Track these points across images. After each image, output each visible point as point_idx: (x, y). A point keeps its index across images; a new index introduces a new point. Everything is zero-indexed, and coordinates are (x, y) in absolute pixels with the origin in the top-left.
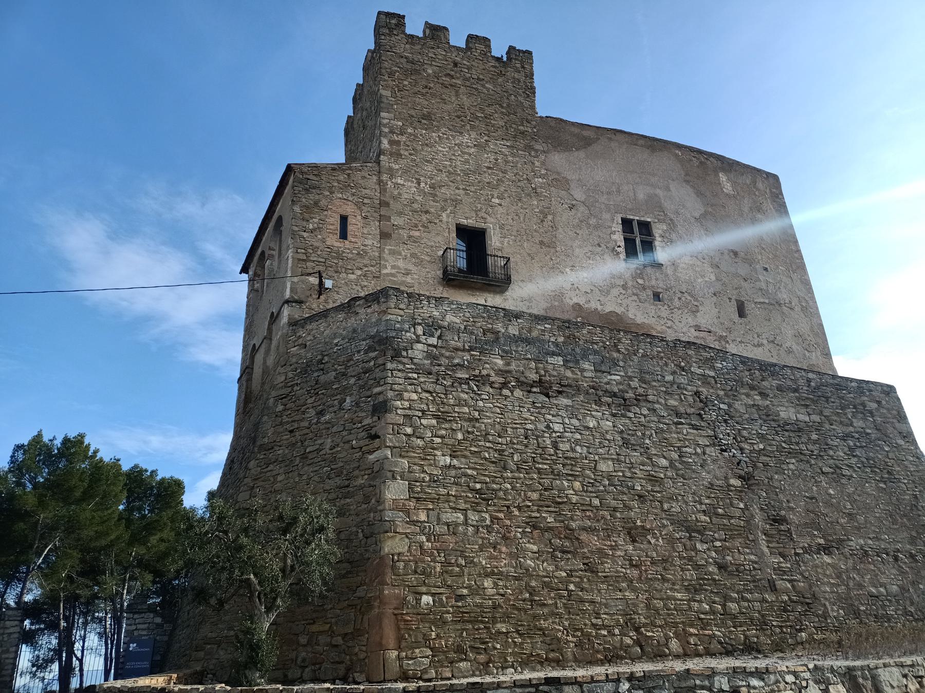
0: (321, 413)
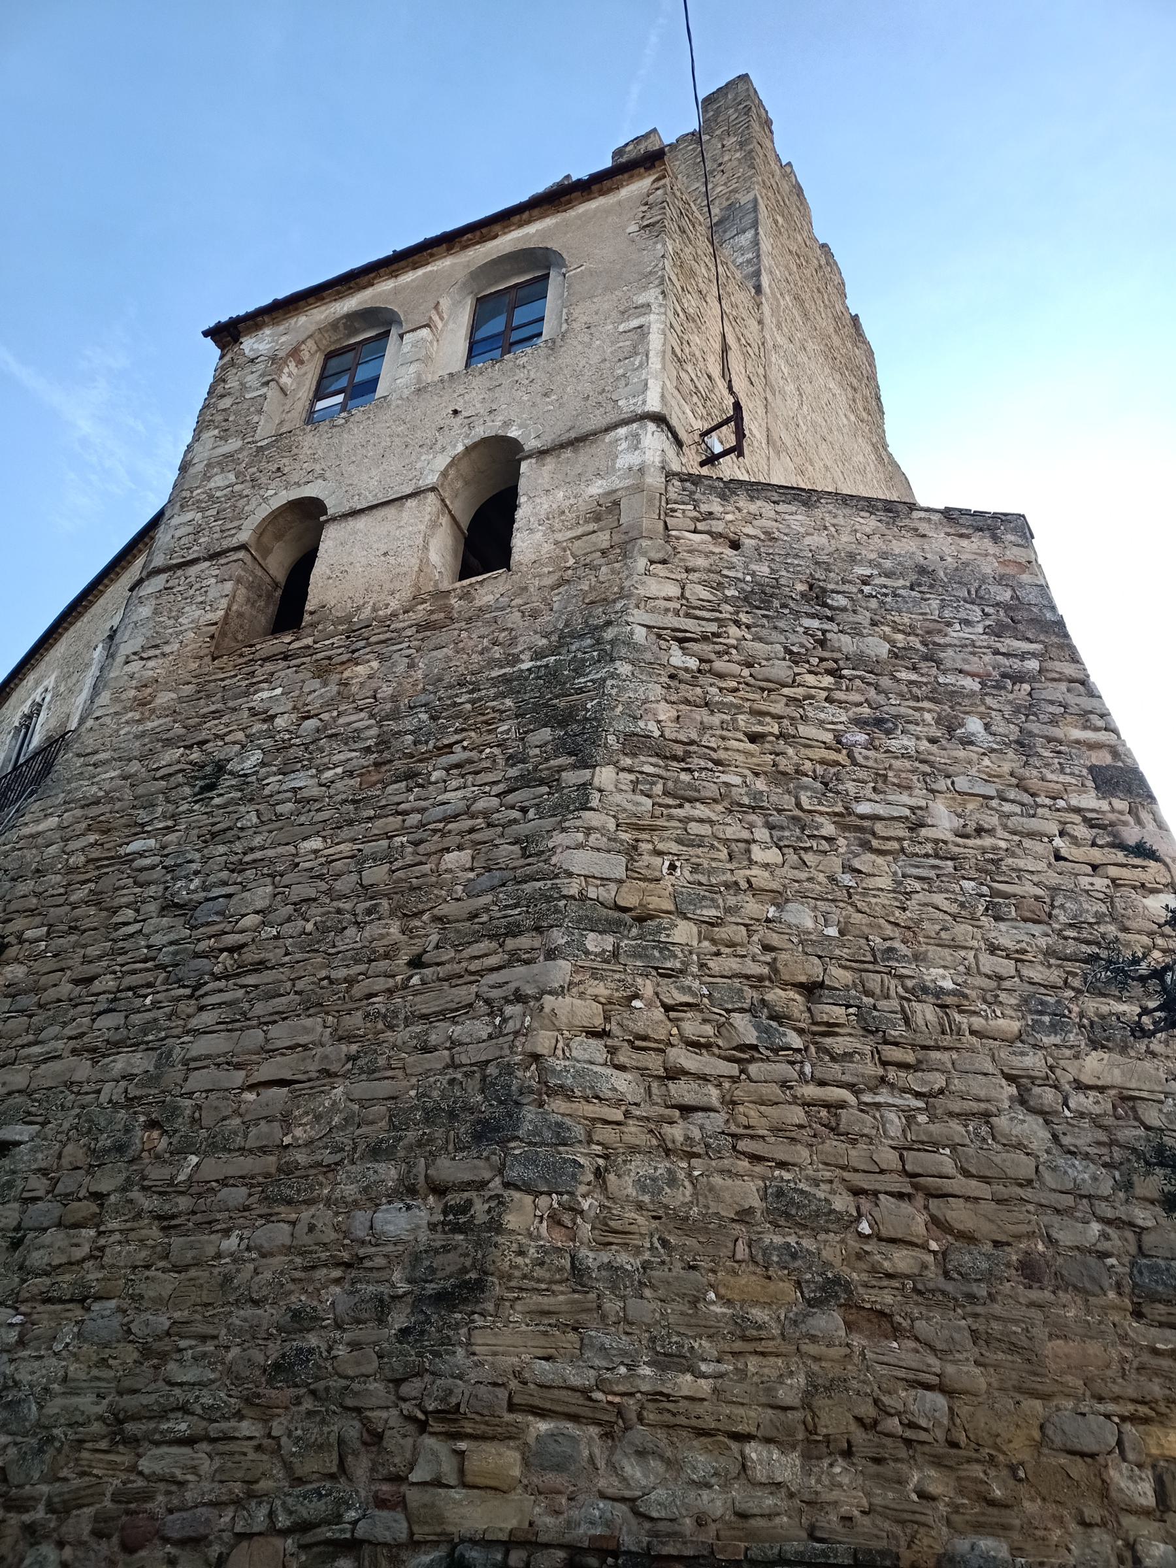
0: (878, 724)
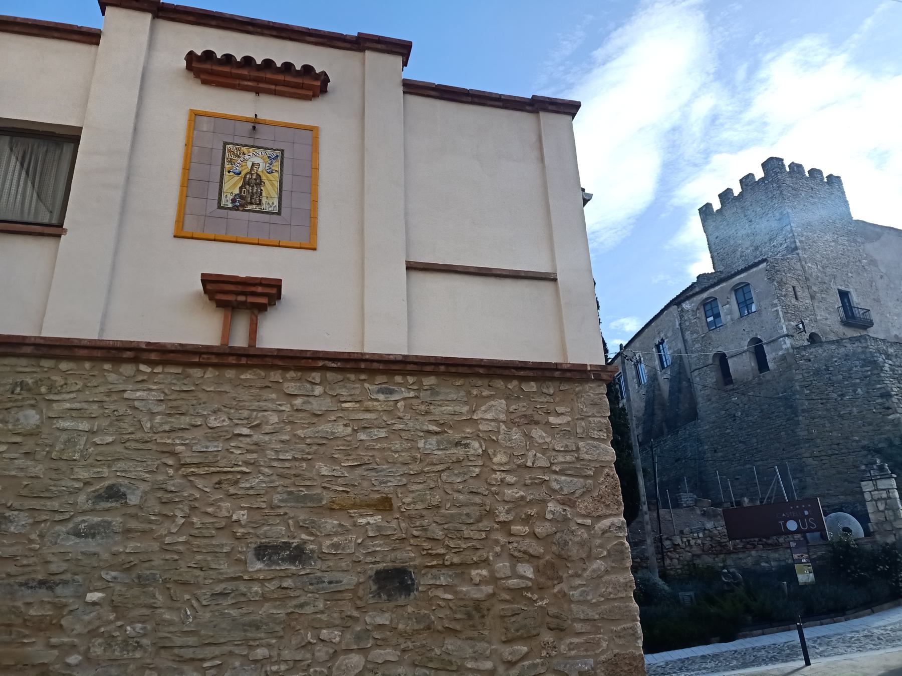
0: (842, 395)
